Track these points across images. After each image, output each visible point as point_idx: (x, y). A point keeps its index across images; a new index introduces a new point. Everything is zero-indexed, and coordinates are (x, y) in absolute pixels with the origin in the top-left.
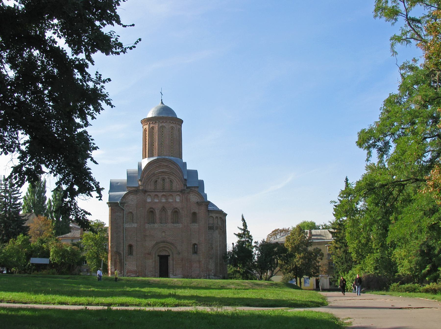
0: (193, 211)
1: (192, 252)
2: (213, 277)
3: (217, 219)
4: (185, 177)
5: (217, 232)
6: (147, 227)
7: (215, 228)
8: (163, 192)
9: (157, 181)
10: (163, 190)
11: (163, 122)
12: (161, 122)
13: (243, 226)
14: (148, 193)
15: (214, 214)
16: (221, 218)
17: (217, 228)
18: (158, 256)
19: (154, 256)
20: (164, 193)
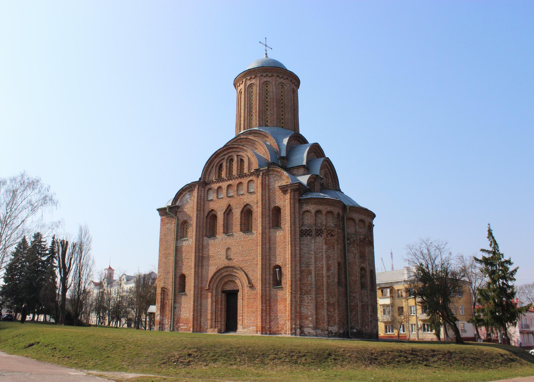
0: (272, 206)
1: (271, 282)
2: (312, 331)
3: (319, 216)
4: (284, 154)
5: (320, 240)
6: (205, 243)
7: (314, 232)
8: (229, 180)
9: (221, 165)
10: (230, 176)
11: (251, 78)
12: (248, 78)
13: (491, 245)
14: (209, 187)
15: (313, 206)
16: (330, 212)
17: (319, 233)
18: (223, 292)
19: (214, 292)
20: (230, 182)
